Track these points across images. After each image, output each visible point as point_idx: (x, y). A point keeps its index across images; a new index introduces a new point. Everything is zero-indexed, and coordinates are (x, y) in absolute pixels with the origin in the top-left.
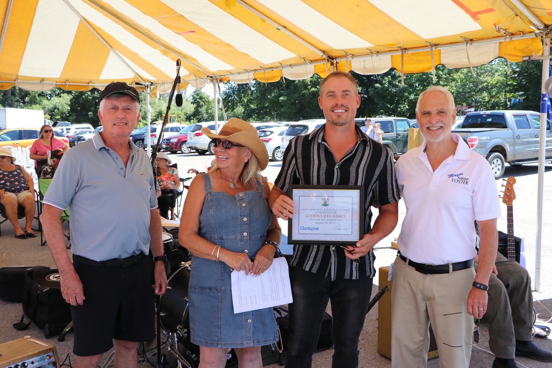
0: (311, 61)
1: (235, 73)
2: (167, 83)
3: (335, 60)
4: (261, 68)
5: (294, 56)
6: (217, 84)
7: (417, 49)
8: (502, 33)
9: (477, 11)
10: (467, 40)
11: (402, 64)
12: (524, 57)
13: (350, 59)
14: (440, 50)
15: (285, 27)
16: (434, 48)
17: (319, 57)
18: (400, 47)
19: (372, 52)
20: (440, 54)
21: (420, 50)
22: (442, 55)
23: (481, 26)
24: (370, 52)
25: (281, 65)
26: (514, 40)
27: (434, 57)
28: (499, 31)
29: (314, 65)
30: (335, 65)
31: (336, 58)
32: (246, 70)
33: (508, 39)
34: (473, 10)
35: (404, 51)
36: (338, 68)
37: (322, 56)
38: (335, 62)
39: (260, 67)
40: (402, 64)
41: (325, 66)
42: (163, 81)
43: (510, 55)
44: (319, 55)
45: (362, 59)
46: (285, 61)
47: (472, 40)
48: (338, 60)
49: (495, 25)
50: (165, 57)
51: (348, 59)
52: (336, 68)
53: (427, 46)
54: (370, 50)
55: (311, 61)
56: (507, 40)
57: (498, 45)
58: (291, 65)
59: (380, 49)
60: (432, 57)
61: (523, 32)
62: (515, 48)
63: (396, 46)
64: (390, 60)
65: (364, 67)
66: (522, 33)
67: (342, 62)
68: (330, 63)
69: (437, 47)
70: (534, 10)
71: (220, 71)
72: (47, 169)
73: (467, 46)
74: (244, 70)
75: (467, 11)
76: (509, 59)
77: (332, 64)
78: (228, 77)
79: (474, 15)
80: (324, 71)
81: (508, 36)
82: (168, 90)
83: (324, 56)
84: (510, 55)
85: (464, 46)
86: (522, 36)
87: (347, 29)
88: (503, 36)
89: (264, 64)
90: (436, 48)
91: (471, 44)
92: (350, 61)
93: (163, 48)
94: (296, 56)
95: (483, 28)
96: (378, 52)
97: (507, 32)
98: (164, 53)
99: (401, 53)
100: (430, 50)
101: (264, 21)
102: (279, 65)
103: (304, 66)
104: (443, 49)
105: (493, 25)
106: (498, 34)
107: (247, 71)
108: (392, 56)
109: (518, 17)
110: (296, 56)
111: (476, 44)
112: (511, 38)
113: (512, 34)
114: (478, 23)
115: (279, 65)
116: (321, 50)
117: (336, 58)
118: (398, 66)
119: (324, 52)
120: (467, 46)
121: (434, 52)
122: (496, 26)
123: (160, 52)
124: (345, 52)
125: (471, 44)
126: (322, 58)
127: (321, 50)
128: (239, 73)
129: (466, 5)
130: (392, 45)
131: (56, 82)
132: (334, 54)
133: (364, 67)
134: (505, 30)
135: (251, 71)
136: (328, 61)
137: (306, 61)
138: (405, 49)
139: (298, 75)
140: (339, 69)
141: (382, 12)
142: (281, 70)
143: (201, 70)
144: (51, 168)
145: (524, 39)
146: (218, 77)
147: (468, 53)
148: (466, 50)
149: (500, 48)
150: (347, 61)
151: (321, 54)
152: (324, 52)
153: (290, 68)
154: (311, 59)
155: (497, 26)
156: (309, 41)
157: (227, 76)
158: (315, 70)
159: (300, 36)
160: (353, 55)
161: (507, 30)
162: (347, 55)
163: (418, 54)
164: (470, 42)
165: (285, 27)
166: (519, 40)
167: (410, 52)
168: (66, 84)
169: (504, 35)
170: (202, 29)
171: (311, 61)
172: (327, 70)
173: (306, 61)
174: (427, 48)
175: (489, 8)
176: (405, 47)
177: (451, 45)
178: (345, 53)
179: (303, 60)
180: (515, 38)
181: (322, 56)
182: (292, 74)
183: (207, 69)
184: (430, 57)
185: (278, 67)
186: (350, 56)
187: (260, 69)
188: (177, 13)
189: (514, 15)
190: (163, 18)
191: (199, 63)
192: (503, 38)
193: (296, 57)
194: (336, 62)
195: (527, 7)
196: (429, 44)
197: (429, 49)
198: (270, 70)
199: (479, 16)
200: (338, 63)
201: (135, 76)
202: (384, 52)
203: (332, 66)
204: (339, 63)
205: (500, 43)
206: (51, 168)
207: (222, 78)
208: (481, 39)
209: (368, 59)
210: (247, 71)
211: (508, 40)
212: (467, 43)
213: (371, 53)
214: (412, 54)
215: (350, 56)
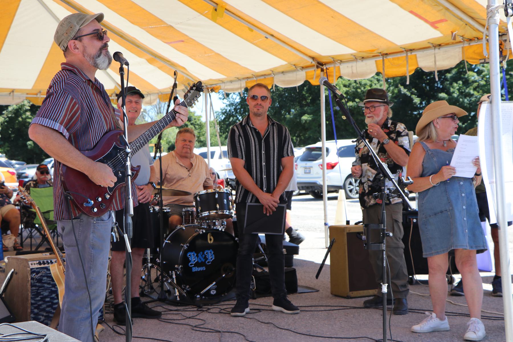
0: (303, 68)
1: (227, 82)
2: (153, 94)
3: (324, 66)
4: (253, 76)
5: (284, 63)
6: (208, 94)
7: (395, 54)
8: (459, 39)
9: (434, 21)
10: (434, 45)
11: (384, 69)
12: (480, 60)
13: (338, 65)
14: (416, 55)
15: (272, 35)
16: (409, 54)
17: (309, 64)
18: (380, 53)
19: (356, 57)
20: (416, 58)
21: (399, 56)
22: (419, 59)
23: (441, 32)
24: (354, 57)
25: (273, 73)
26: (472, 45)
27: (409, 61)
28: (454, 39)
29: (306, 72)
30: (325, 71)
31: (325, 64)
32: (238, 78)
33: (467, 44)
34: (432, 20)
35: (385, 56)
36: (328, 74)
37: (312, 62)
38: (325, 68)
39: (252, 75)
40: (384, 69)
41: (313, 73)
42: (148, 92)
43: (471, 58)
44: (309, 62)
45: (349, 65)
46: (276, 68)
47: (440, 45)
48: (328, 66)
49: (452, 33)
50: (151, 67)
51: (337, 65)
52: (326, 74)
53: (402, 52)
54: (354, 56)
55: (303, 68)
56: (465, 45)
57: (461, 50)
58: (283, 72)
59: (364, 55)
60: (407, 62)
61: (478, 38)
62: (474, 52)
63: (375, 52)
64: (375, 65)
65: (353, 73)
66: (476, 39)
67: (331, 67)
68: (320, 69)
69: (412, 52)
70: (478, 20)
71: (211, 80)
72: (30, 184)
73: (435, 51)
74: (236, 79)
75: (426, 21)
76: (470, 61)
77: (322, 70)
78: (220, 86)
79: (433, 24)
80: (312, 78)
81: (466, 42)
82: (153, 102)
83: (314, 63)
84: (471, 58)
85: (431, 51)
86: (476, 41)
87: (329, 37)
88: (460, 42)
89: (255, 72)
90: (411, 53)
91: (439, 49)
92: (339, 67)
93: (150, 56)
94: (286, 63)
95: (444, 35)
96: (363, 58)
97: (465, 38)
98: (150, 61)
99: (382, 59)
100: (405, 55)
101: (252, 30)
102: (271, 72)
103: (295, 74)
104: (419, 54)
105: (451, 33)
106: (454, 41)
107: (239, 79)
108: (376, 61)
109: (467, 26)
110: (286, 63)
111: (443, 49)
112: (470, 43)
113: (471, 40)
114: (438, 30)
115: (271, 72)
116: (310, 57)
117: (325, 64)
118: (381, 71)
119: (313, 58)
120: (435, 51)
121: (409, 57)
122: (452, 33)
123: (146, 61)
124: (333, 58)
125: (439, 49)
126: (312, 64)
127: (310, 57)
128: (231, 82)
129: (424, 16)
130: (373, 51)
131: (27, 94)
132: (323, 61)
133: (353, 73)
134: (462, 36)
135: (244, 79)
136: (317, 67)
137: (297, 68)
138: (386, 54)
139: (290, 82)
140: (329, 76)
141: (355, 23)
142: (273, 77)
143: (191, 79)
144: (35, 183)
145: (478, 44)
146: (209, 86)
147: (437, 58)
148: (433, 56)
149: (463, 52)
150: (335, 67)
151: (311, 60)
152: (313, 58)
153: (282, 74)
154: (302, 65)
155: (454, 33)
156: (297, 48)
157: (218, 85)
158: (306, 76)
159: (288, 43)
160: (341, 61)
161: (465, 37)
162: (335, 61)
163: (398, 58)
164: (438, 47)
165: (272, 35)
166: (476, 45)
167: (390, 57)
168: (38, 96)
169: (462, 40)
170: (191, 39)
171: (303, 68)
172: (315, 77)
173: (296, 68)
174: (402, 53)
175: (442, 18)
176: (385, 52)
177: (423, 50)
178: (332, 59)
179: (294, 67)
180: (473, 43)
181: (312, 62)
182: (283, 82)
183: (197, 78)
184: (405, 62)
185: (270, 74)
186: (339, 62)
187: (253, 77)
188: (166, 24)
189: (464, 24)
190: (152, 28)
191: (188, 72)
192: (462, 44)
193: (286, 64)
194: (326, 68)
195: (472, 18)
196: (404, 50)
197: (404, 55)
198: (263, 77)
199: (437, 25)
200: (328, 69)
201: (115, 86)
202: (368, 58)
203: (322, 73)
204: (329, 69)
205: (463, 48)
206: (35, 183)
207: (214, 88)
208: (447, 44)
209: (354, 64)
210: (239, 79)
211: (467, 45)
212: (435, 49)
213: (355, 58)
214: (393, 59)
215: (339, 62)
